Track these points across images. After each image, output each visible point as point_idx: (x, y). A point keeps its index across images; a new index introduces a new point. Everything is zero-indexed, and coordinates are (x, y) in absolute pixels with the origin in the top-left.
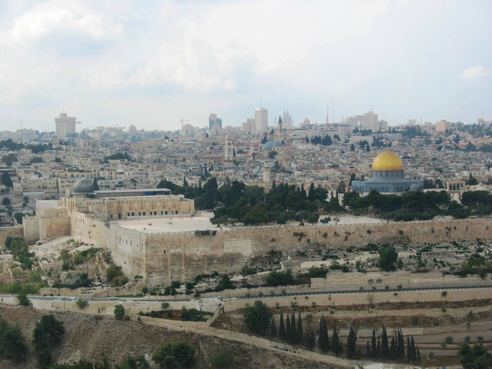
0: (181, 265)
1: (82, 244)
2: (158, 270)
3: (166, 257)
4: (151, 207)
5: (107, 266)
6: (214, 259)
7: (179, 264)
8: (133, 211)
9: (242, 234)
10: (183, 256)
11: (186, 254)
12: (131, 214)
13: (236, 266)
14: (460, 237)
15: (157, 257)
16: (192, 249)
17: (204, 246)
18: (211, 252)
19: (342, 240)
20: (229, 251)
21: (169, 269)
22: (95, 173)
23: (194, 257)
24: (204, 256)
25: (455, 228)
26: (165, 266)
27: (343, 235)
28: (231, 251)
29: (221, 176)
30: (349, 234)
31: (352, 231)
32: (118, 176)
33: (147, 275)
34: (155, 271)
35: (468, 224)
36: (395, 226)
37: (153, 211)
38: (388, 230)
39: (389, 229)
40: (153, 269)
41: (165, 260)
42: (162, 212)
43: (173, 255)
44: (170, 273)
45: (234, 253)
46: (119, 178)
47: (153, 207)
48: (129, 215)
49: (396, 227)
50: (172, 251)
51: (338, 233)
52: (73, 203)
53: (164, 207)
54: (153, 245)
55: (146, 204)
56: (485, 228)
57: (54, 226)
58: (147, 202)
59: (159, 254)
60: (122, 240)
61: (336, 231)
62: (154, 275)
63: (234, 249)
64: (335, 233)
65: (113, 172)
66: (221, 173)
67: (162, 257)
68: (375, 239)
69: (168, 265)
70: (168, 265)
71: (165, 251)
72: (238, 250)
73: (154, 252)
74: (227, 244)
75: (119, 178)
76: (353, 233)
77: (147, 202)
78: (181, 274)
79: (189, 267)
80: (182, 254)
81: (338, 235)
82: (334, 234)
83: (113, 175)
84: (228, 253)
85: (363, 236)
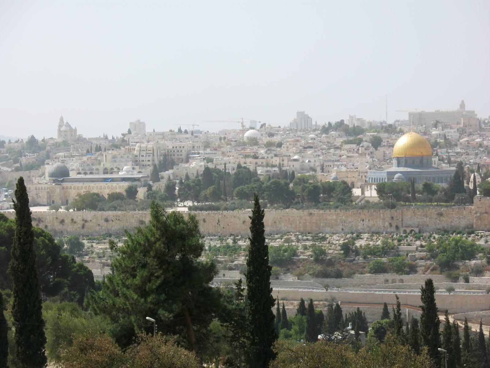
14: (210, 231)
19: (79, 227)
25: (204, 221)
27: (80, 223)
30: (86, 221)
31: (89, 219)
32: (291, 163)
35: (220, 216)
36: (135, 216)
38: (127, 220)
39: (128, 219)
49: (137, 217)
51: (75, 220)
56: (242, 222)
58: (95, 189)
61: (73, 218)
64: (72, 220)
65: (286, 159)
68: (113, 229)
75: (292, 166)
76: (91, 221)
77: (95, 189)
81: (75, 222)
82: (71, 222)
83: (285, 162)
85: (101, 224)
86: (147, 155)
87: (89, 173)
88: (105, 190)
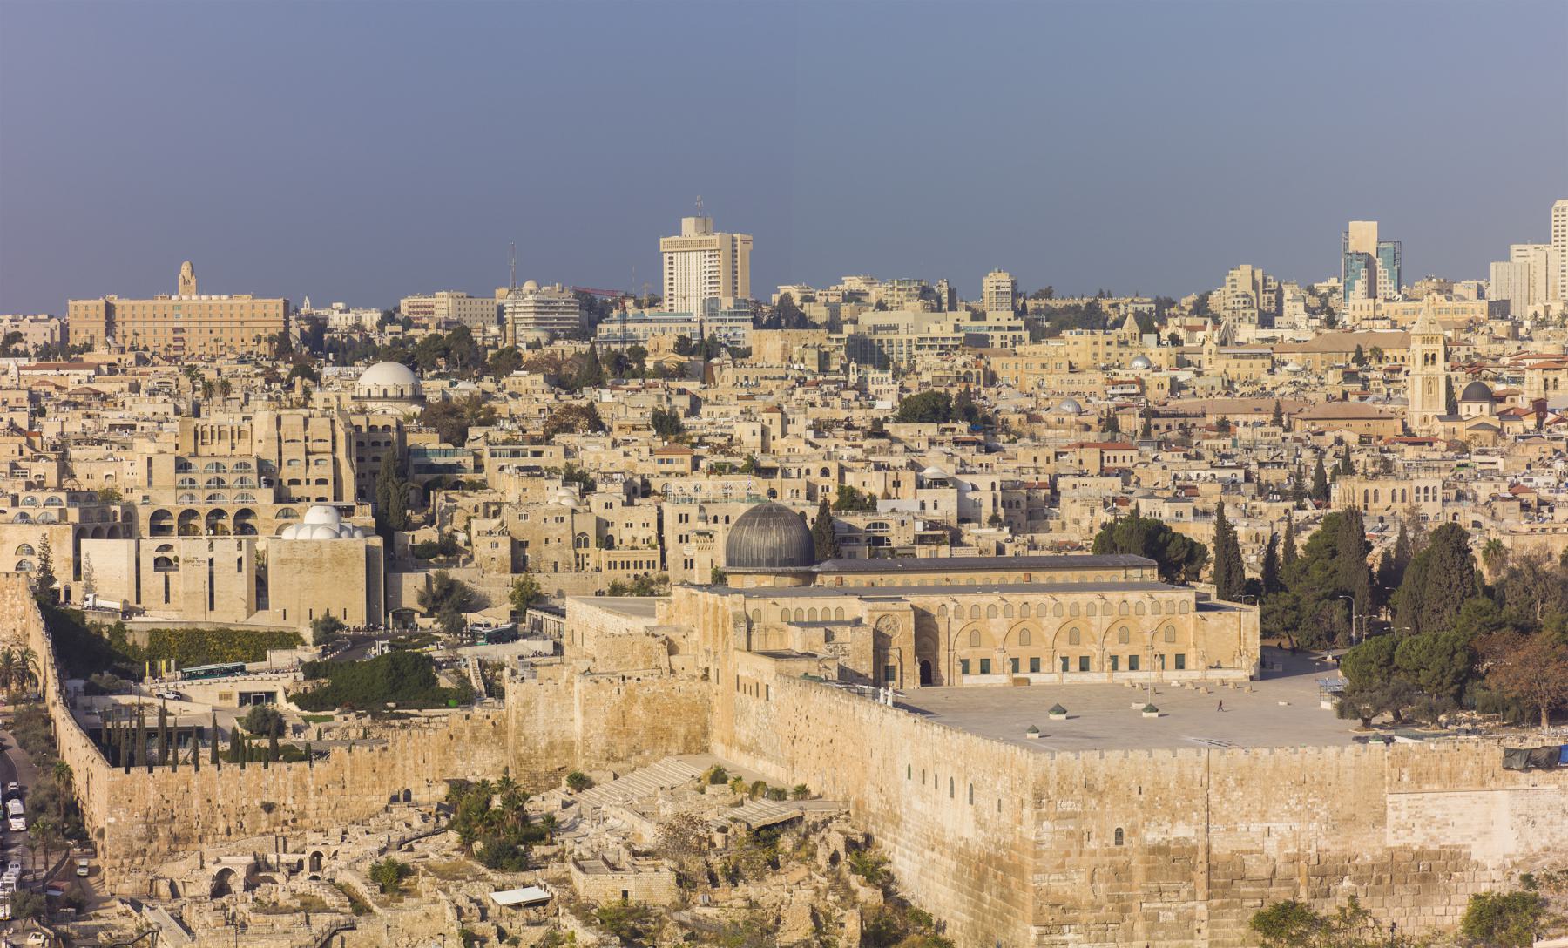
0: (1193, 895)
1: (757, 788)
2: (1085, 916)
3: (1122, 859)
4: (1065, 634)
5: (869, 895)
6: (1342, 873)
7: (1184, 893)
8: (983, 652)
9: (1470, 763)
10: (1201, 855)
11: (1214, 851)
12: (975, 666)
13: (1440, 910)
15: (1085, 857)
16: (1242, 826)
17: (1292, 813)
18: (1324, 843)
20: (1408, 840)
21: (1136, 912)
22: (824, 481)
23: (1251, 861)
24: (1294, 860)
26: (1120, 898)
28: (1417, 840)
29: (1385, 500)
33: (1041, 935)
34: (1075, 921)
37: (1075, 653)
40: (1065, 910)
41: (1121, 874)
42: (1114, 659)
43: (1157, 850)
44: (1139, 927)
45: (1433, 847)
46: (930, 506)
47: (1074, 639)
48: (965, 671)
50: (1153, 836)
52: (724, 610)
53: (1124, 638)
54: (1068, 806)
55: (1045, 622)
57: (638, 711)
58: (1050, 614)
59: (1092, 845)
60: (930, 779)
62: (1069, 937)
63: (1434, 831)
66: (1385, 487)
67: (1107, 859)
69: (1132, 898)
70: (1132, 898)
71: (1119, 833)
72: (1451, 838)
73: (1070, 834)
74: (1400, 806)
77: (1050, 614)
78: (1192, 937)
79: (1227, 905)
80: (1195, 849)
84: (1404, 848)
86: (312, 459)
87: (106, 532)
88: (1095, 621)
